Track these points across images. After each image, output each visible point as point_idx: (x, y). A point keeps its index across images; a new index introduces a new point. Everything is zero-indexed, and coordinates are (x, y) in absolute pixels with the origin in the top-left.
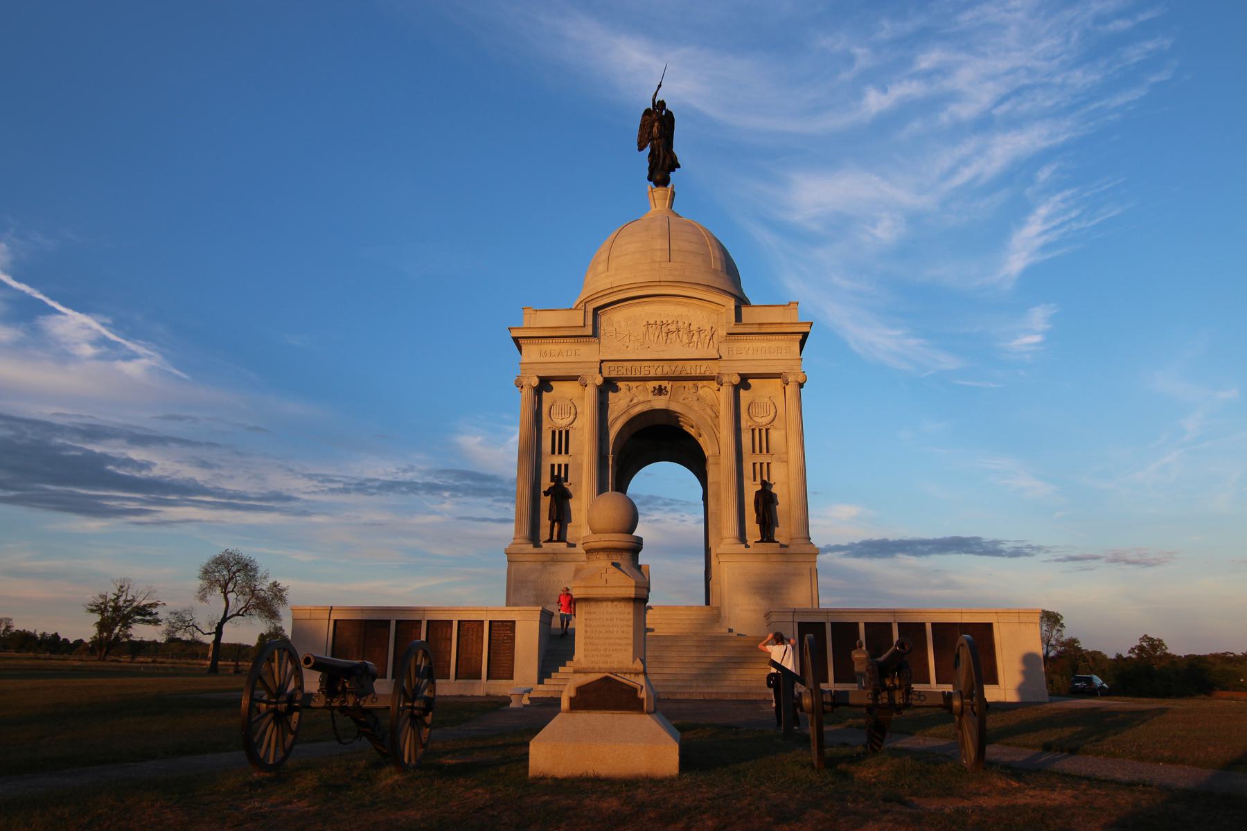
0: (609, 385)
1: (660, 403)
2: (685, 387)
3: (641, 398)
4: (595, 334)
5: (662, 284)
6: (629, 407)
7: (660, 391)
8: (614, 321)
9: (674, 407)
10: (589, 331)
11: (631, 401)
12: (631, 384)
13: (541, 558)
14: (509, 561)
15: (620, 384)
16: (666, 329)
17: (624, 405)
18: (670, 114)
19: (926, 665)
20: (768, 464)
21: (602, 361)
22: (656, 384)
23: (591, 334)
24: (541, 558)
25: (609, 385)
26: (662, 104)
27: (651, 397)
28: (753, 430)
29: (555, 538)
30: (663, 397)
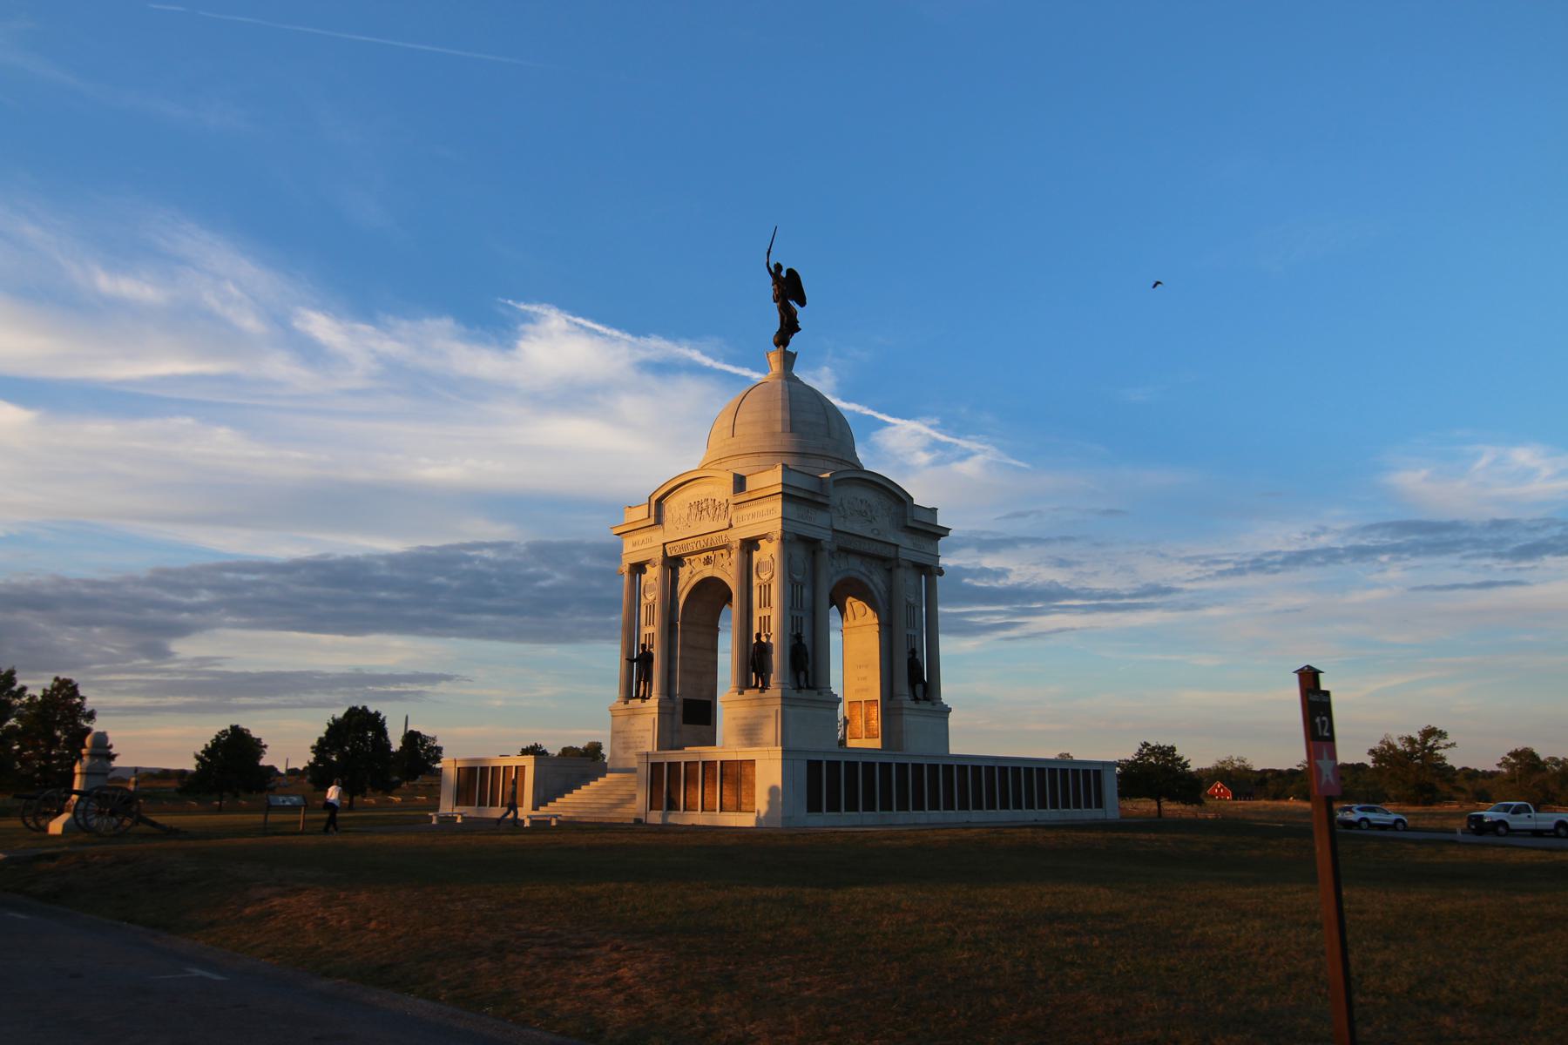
0: (673, 564)
1: (708, 572)
2: (722, 555)
3: (698, 569)
4: (659, 521)
5: (723, 460)
6: (690, 578)
7: (708, 561)
8: (673, 506)
9: (718, 574)
10: (652, 521)
11: (691, 573)
12: (692, 558)
13: (627, 712)
14: (613, 716)
15: (686, 559)
16: (699, 508)
17: (688, 577)
18: (791, 272)
19: (716, 798)
20: (769, 617)
21: (664, 544)
22: (704, 555)
23: (653, 523)
24: (627, 712)
25: (673, 564)
26: (779, 267)
27: (702, 567)
28: (761, 587)
29: (641, 694)
30: (710, 566)
